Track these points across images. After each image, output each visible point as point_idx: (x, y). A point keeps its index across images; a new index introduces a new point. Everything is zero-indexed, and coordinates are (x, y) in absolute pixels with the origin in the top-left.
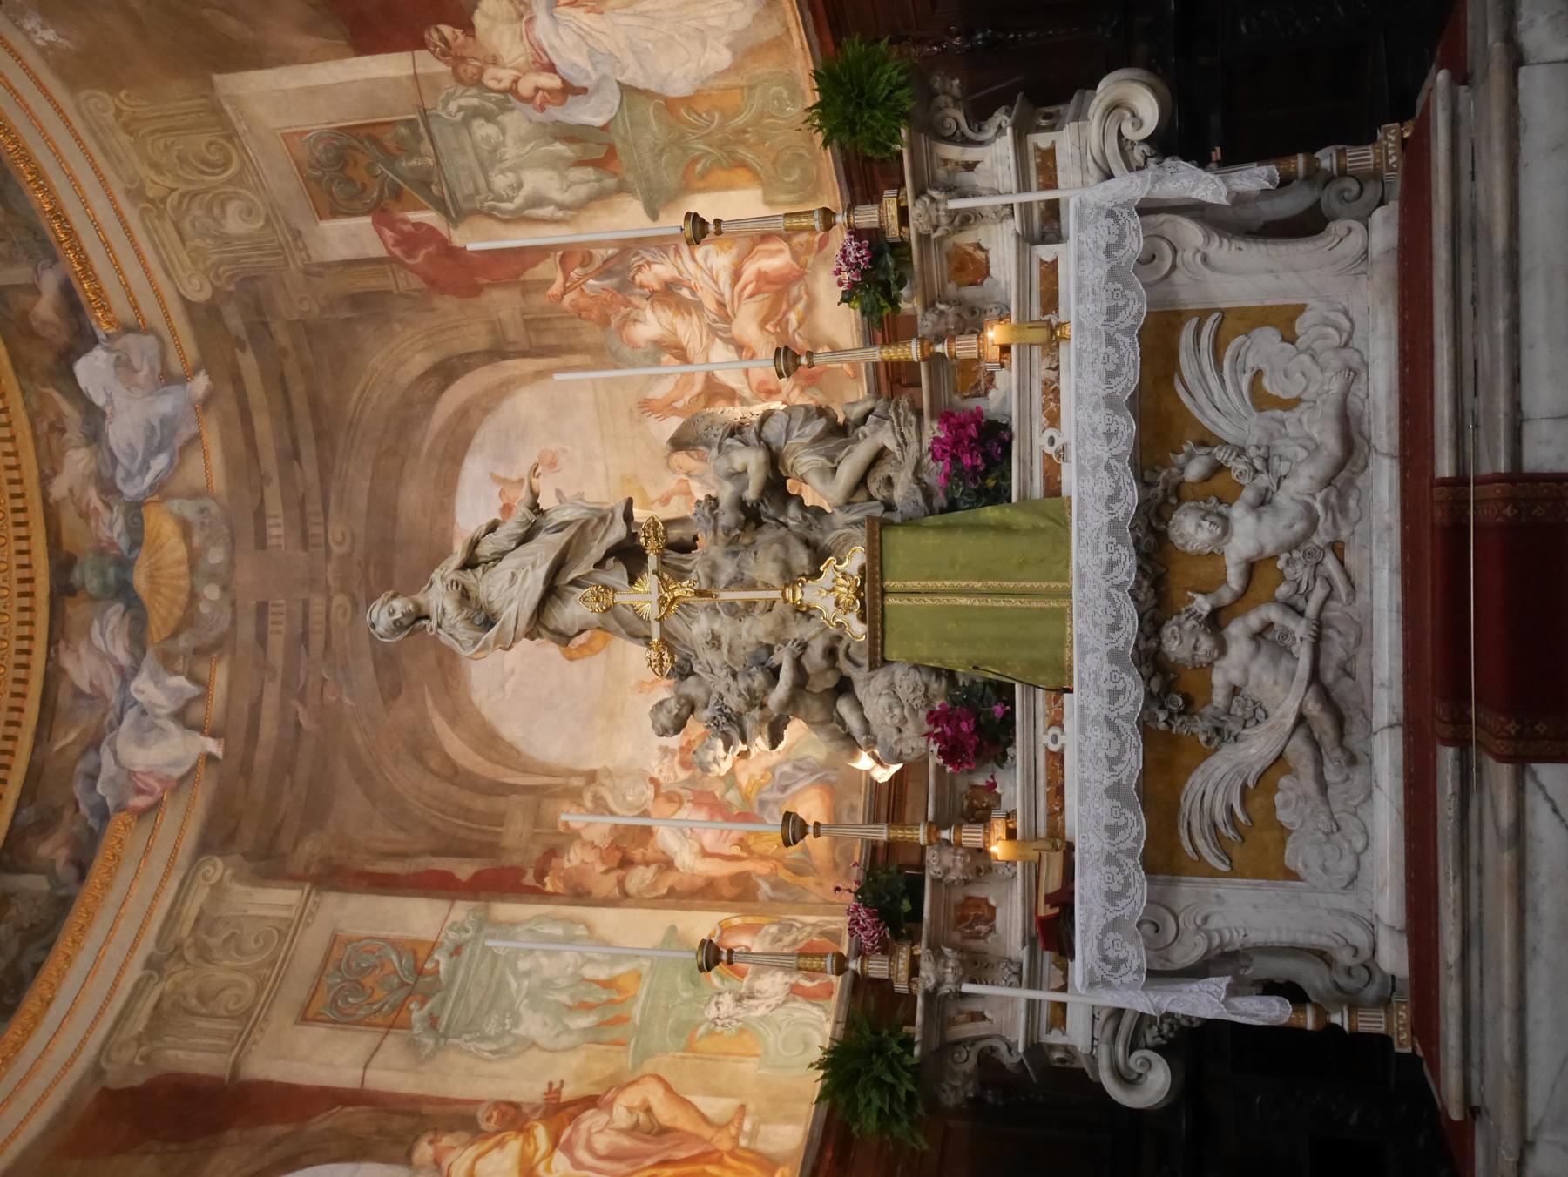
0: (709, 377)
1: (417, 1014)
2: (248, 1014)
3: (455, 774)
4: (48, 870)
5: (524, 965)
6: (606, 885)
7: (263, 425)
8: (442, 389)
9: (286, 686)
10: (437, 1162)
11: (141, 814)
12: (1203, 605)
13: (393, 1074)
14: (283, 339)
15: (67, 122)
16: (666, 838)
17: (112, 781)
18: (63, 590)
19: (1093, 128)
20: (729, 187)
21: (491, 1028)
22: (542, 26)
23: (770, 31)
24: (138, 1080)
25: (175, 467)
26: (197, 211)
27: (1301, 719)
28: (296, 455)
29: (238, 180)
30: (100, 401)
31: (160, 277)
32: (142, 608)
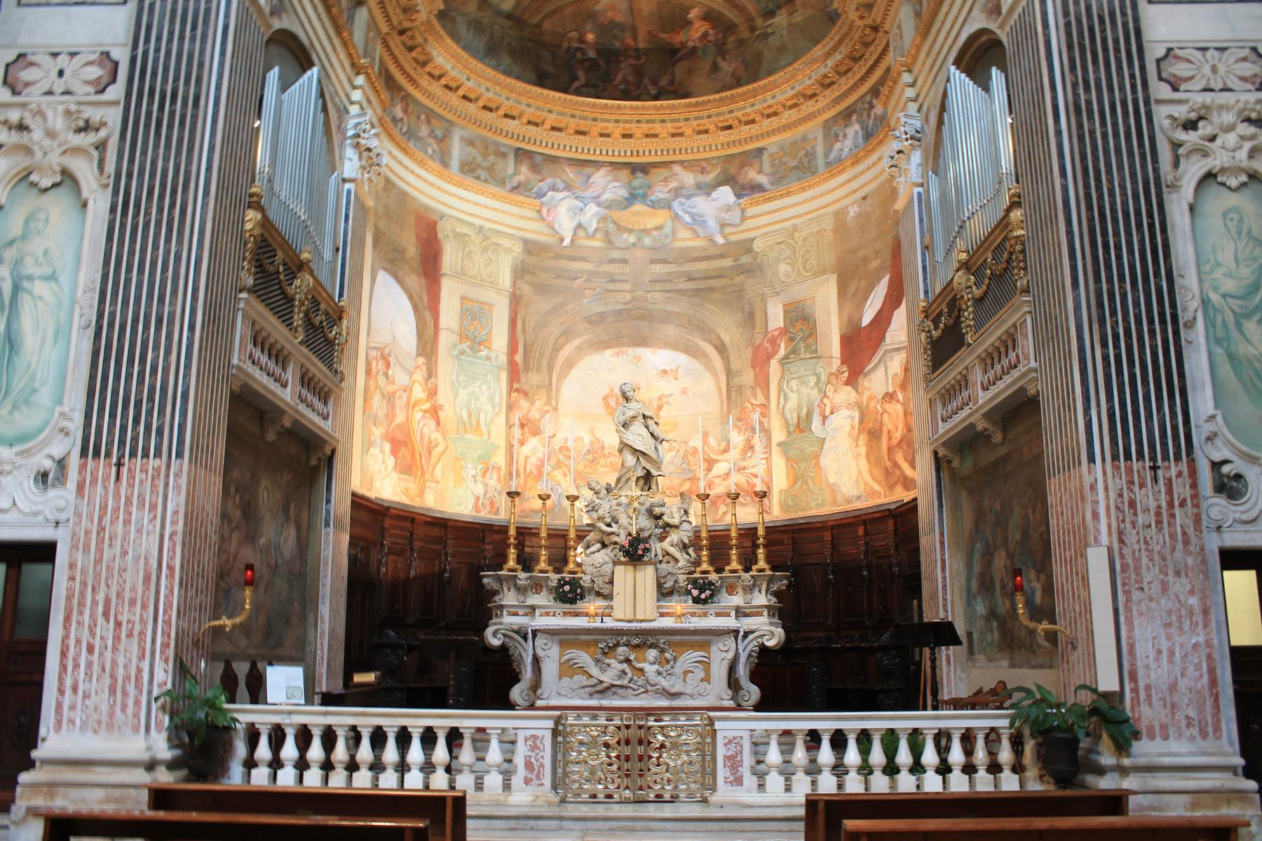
0: (716, 461)
1: (465, 346)
2: (463, 274)
3: (557, 349)
4: (516, 173)
5: (484, 387)
6: (516, 417)
7: (702, 266)
8: (715, 347)
9: (592, 273)
10: (417, 367)
11: (539, 212)
12: (632, 658)
13: (446, 339)
14: (738, 279)
15: (822, 208)
16: (533, 442)
17: (553, 199)
18: (635, 169)
19: (767, 628)
20: (788, 476)
21: (461, 378)
22: (845, 413)
23: (839, 499)
24: (440, 235)
25: (686, 225)
26: (788, 252)
27: (602, 682)
28: (690, 280)
29: (799, 274)
30: (714, 195)
31: (764, 230)
32: (625, 208)
